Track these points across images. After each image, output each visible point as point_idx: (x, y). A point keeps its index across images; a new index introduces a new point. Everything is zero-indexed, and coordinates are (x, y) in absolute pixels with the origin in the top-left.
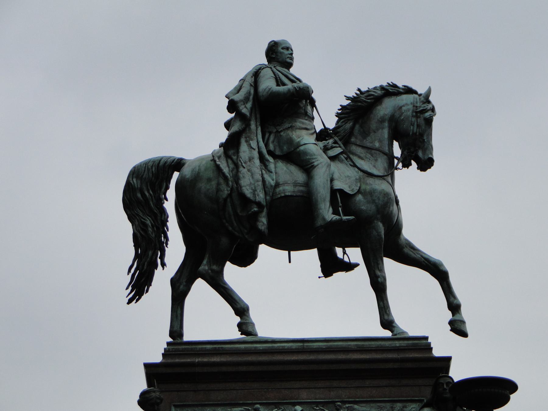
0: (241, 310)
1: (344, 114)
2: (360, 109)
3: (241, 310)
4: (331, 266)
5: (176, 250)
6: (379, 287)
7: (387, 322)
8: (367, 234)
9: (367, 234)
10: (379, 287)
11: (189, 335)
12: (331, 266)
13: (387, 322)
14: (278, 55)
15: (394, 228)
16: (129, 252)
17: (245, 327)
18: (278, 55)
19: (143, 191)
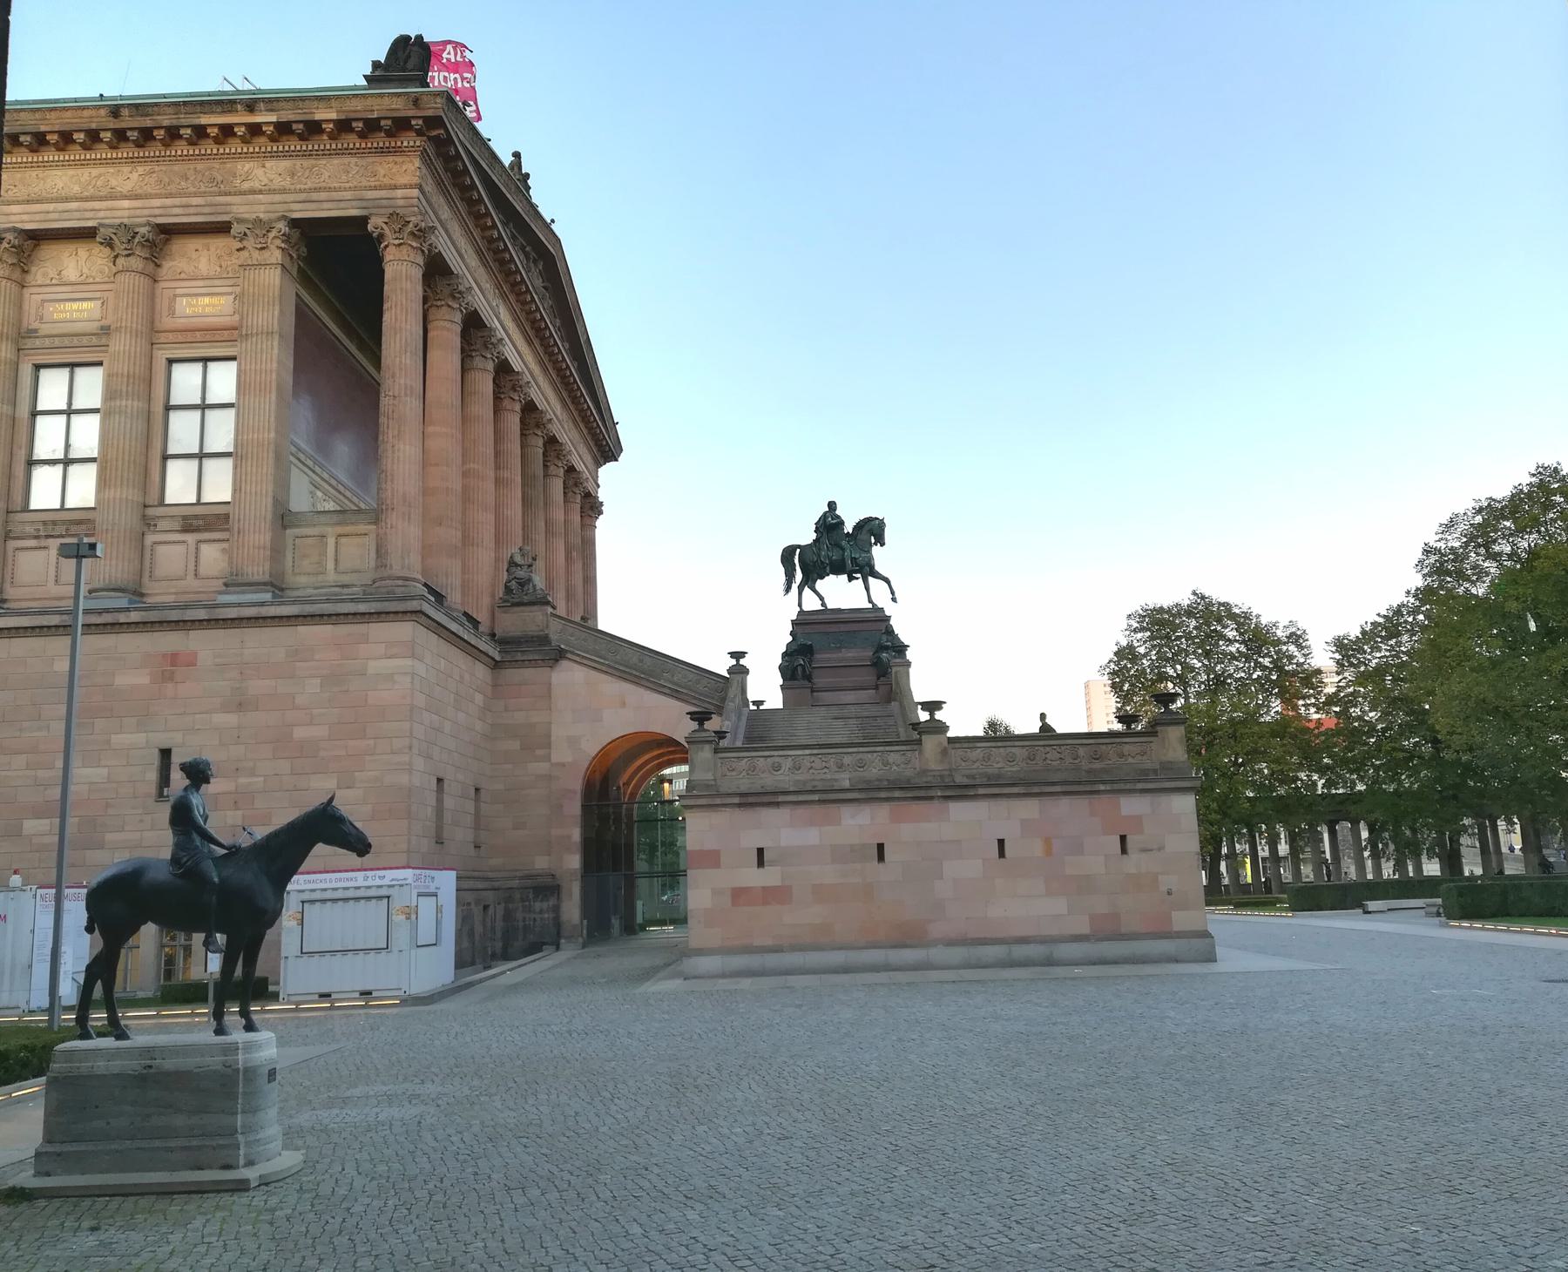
0: (822, 599)
1: (855, 528)
2: (860, 526)
3: (822, 599)
4: (851, 579)
5: (799, 576)
6: (867, 589)
7: (870, 601)
8: (864, 569)
9: (864, 569)
10: (867, 589)
11: (806, 608)
12: (851, 579)
13: (870, 601)
14: (832, 506)
15: (872, 567)
16: (784, 578)
17: (823, 604)
18: (832, 505)
19: (787, 555)
